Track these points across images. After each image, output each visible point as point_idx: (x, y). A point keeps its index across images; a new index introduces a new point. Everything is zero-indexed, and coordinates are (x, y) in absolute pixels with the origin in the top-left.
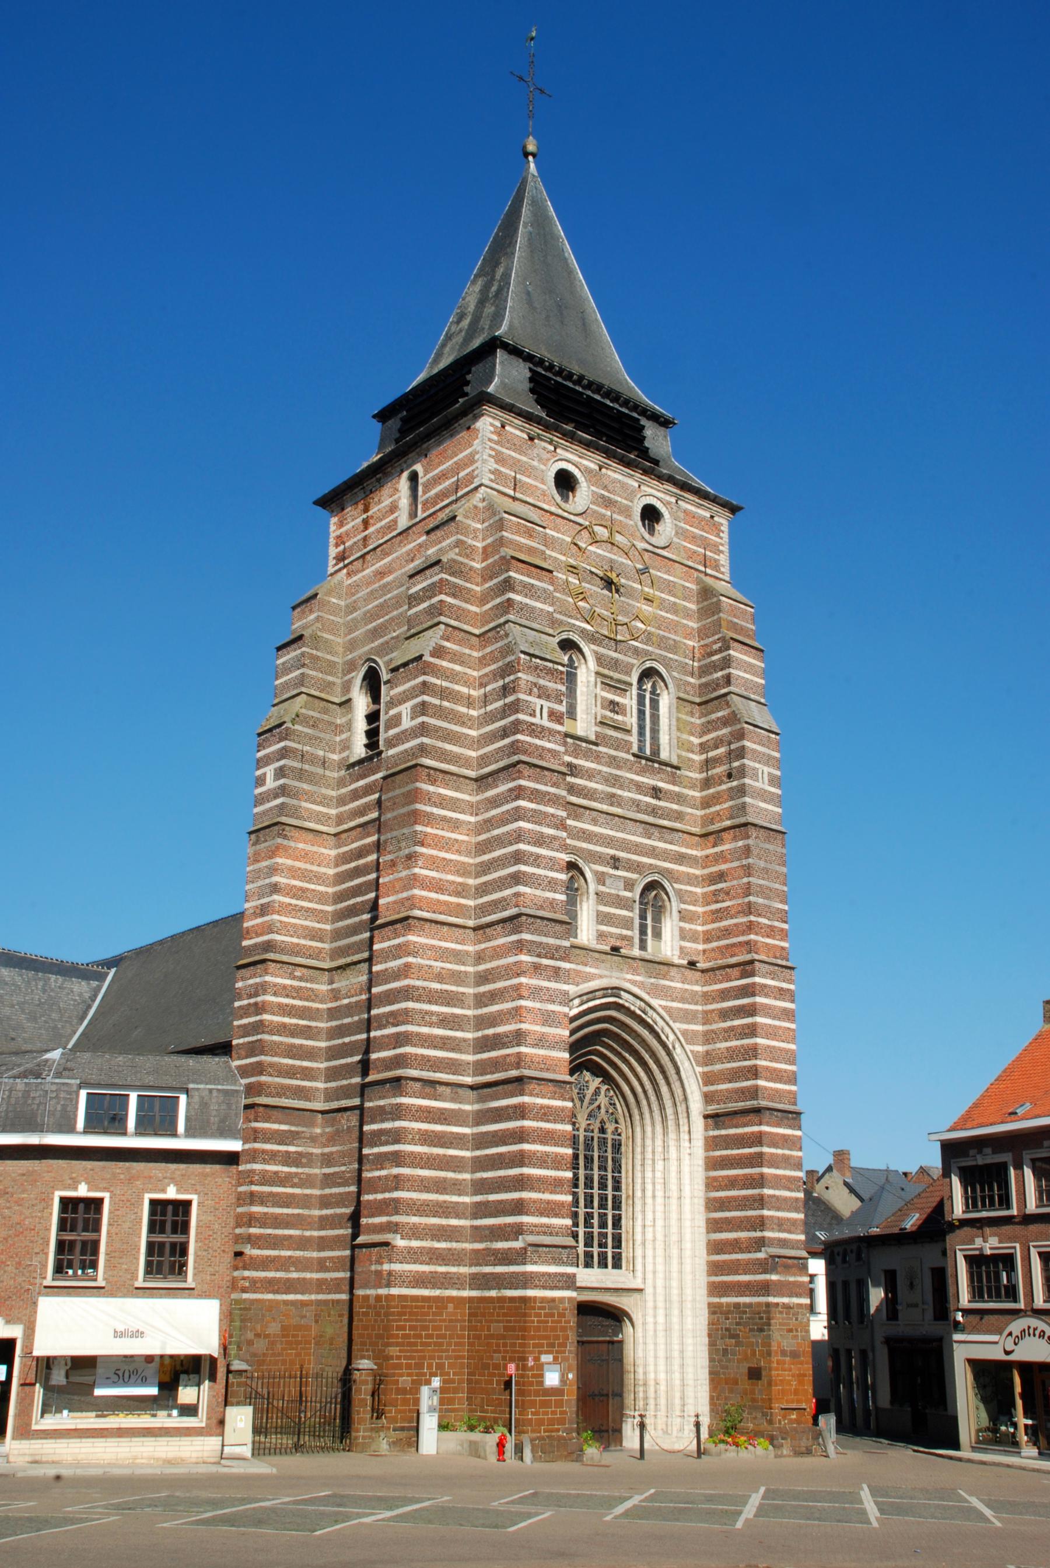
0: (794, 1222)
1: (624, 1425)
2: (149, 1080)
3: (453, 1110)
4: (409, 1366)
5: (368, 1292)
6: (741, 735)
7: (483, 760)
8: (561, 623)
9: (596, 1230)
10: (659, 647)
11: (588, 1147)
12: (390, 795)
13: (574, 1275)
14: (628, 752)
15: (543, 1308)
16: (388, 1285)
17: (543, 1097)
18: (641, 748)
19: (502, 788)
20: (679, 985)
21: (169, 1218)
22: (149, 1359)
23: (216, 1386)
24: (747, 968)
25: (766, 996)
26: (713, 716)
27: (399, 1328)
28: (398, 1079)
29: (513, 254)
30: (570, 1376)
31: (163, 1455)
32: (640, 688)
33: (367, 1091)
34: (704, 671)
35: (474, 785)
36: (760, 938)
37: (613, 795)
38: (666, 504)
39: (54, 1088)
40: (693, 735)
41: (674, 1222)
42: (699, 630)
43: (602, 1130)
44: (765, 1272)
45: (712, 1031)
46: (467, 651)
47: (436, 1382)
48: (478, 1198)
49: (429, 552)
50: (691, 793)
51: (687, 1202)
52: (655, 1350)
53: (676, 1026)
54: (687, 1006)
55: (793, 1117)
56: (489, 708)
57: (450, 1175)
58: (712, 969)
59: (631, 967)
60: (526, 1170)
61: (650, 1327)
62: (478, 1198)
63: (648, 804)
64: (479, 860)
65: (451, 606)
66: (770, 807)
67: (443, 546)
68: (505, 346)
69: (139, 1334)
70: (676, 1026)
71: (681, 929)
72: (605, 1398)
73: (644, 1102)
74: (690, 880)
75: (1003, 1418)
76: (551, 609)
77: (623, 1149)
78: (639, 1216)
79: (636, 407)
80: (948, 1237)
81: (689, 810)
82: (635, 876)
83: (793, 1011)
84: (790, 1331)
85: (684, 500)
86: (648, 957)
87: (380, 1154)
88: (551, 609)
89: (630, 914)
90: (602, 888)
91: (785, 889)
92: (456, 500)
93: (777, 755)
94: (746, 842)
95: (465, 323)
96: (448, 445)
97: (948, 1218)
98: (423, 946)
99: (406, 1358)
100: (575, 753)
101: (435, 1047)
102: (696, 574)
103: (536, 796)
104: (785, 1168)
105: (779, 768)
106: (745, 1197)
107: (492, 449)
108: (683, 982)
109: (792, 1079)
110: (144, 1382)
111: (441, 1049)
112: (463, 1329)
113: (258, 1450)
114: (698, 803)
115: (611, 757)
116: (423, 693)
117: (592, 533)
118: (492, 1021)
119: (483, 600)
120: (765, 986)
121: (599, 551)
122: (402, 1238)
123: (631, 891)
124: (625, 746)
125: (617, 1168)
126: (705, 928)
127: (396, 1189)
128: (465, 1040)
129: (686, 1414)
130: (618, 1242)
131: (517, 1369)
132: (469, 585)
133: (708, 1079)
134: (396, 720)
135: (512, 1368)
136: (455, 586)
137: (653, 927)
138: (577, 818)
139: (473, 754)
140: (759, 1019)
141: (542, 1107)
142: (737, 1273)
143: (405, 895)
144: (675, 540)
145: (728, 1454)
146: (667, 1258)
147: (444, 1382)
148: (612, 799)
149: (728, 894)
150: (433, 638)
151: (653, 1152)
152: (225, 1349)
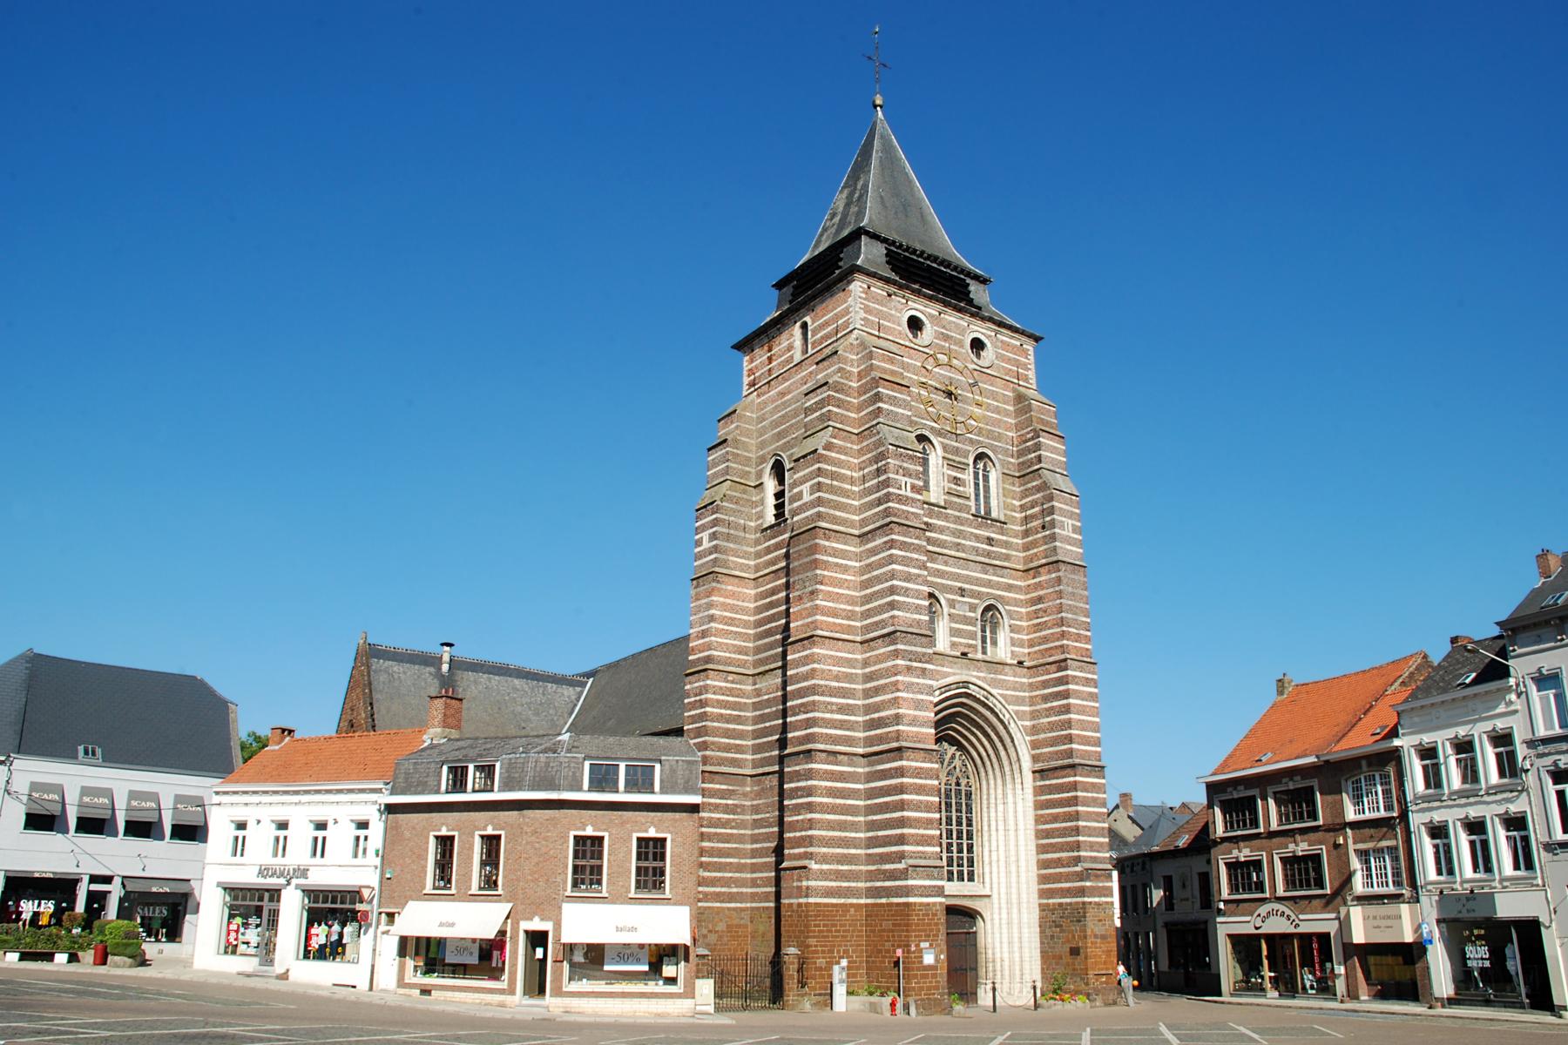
0: (1101, 844)
2: (633, 754)
3: (850, 772)
4: (823, 952)
5: (792, 901)
6: (1051, 498)
7: (864, 522)
8: (916, 423)
9: (955, 855)
10: (988, 438)
11: (948, 796)
12: (796, 549)
13: (943, 887)
14: (968, 513)
15: (921, 910)
16: (807, 896)
18: (978, 509)
19: (879, 541)
20: (1012, 679)
21: (651, 850)
22: (641, 946)
23: (689, 965)
24: (1062, 664)
25: (1077, 684)
26: (1029, 485)
27: (815, 926)
28: (809, 751)
29: (870, 171)
30: (942, 957)
31: (655, 1010)
32: (975, 467)
33: (786, 760)
34: (1021, 454)
35: (858, 540)
36: (1070, 643)
37: (959, 544)
38: (988, 337)
39: (566, 760)
40: (1014, 499)
41: (1012, 847)
42: (1016, 425)
43: (958, 784)
44: (1082, 880)
45: (1037, 711)
46: (849, 445)
47: (844, 963)
48: (871, 834)
49: (819, 377)
50: (1015, 540)
51: (1021, 833)
52: (1001, 938)
53: (1010, 708)
54: (1017, 693)
55: (1099, 770)
56: (867, 485)
57: (849, 818)
58: (1036, 667)
59: (976, 667)
60: (906, 814)
61: (997, 922)
62: (871, 834)
63: (984, 550)
64: (863, 593)
65: (837, 414)
66: (1074, 549)
67: (829, 372)
68: (867, 233)
69: (633, 929)
70: (1010, 708)
71: (1012, 638)
73: (988, 763)
74: (1017, 603)
75: (1252, 973)
76: (910, 413)
77: (973, 796)
78: (986, 844)
79: (962, 271)
80: (1212, 851)
81: (1014, 553)
82: (976, 601)
83: (1096, 694)
84: (1100, 921)
85: (1001, 333)
86: (989, 659)
87: (797, 804)
88: (910, 413)
89: (974, 629)
90: (953, 611)
91: (1087, 606)
92: (837, 340)
93: (1077, 511)
94: (1058, 574)
95: (837, 219)
96: (830, 303)
97: (1212, 837)
98: (824, 656)
99: (821, 946)
100: (930, 515)
101: (836, 728)
102: (1012, 385)
103: (904, 546)
104: (1094, 806)
105: (1079, 521)
106: (1065, 828)
107: (861, 303)
109: (1097, 743)
110: (638, 961)
111: (840, 729)
112: (861, 925)
113: (718, 1009)
114: (1020, 547)
115: (955, 516)
116: (819, 476)
117: (936, 359)
118: (877, 708)
119: (859, 409)
120: (1075, 677)
121: (942, 372)
122: (816, 863)
123: (974, 612)
124: (967, 509)
125: (969, 810)
126: (1029, 637)
127: (810, 829)
128: (857, 722)
130: (971, 862)
131: (903, 953)
132: (848, 399)
133: (1035, 745)
134: (799, 496)
135: (899, 952)
136: (839, 399)
137: (991, 638)
138: (933, 561)
139: (857, 518)
140: (1071, 701)
141: (916, 768)
142: (1060, 882)
143: (810, 620)
144: (996, 362)
145: (1056, 1007)
146: (1008, 873)
147: (849, 962)
148: (958, 546)
149: (1045, 612)
150: (825, 436)
151: (996, 799)
152: (695, 940)
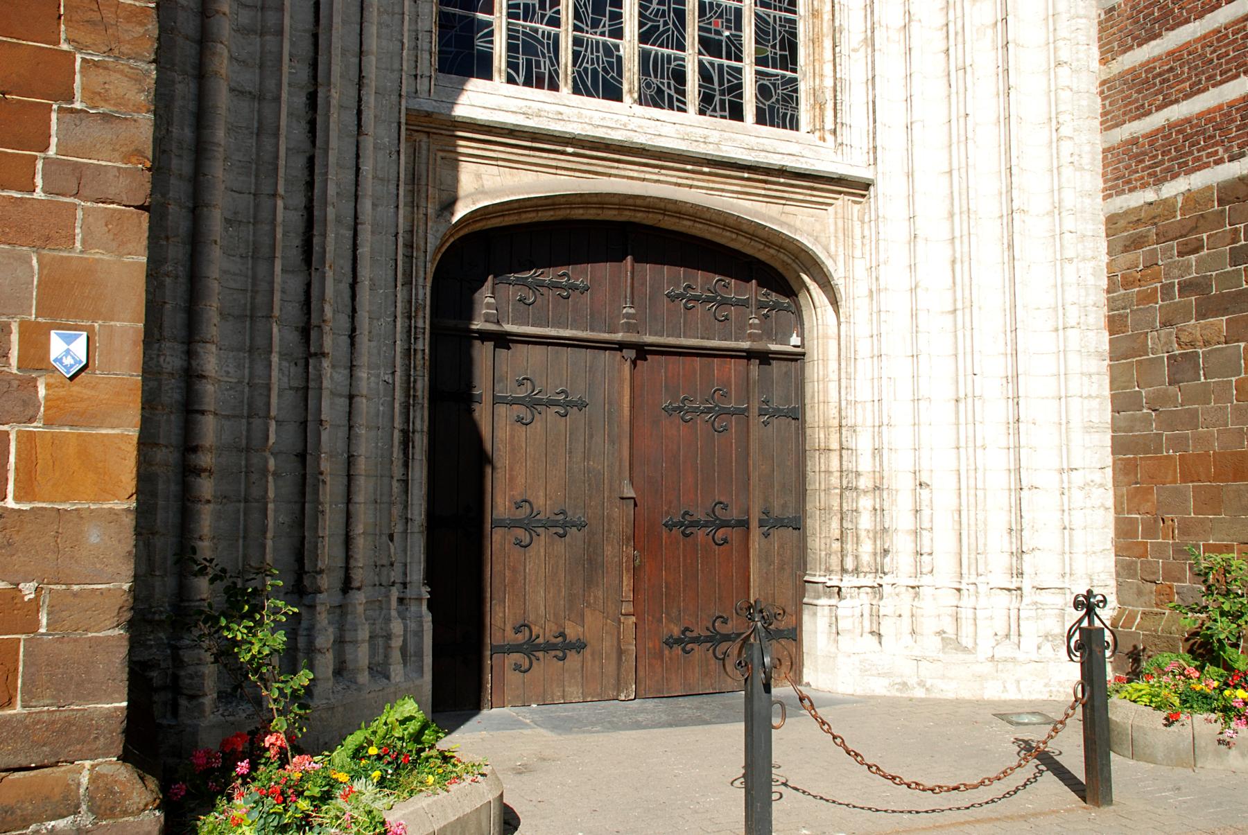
1: (806, 618)
72: (735, 534)
129: (1027, 585)
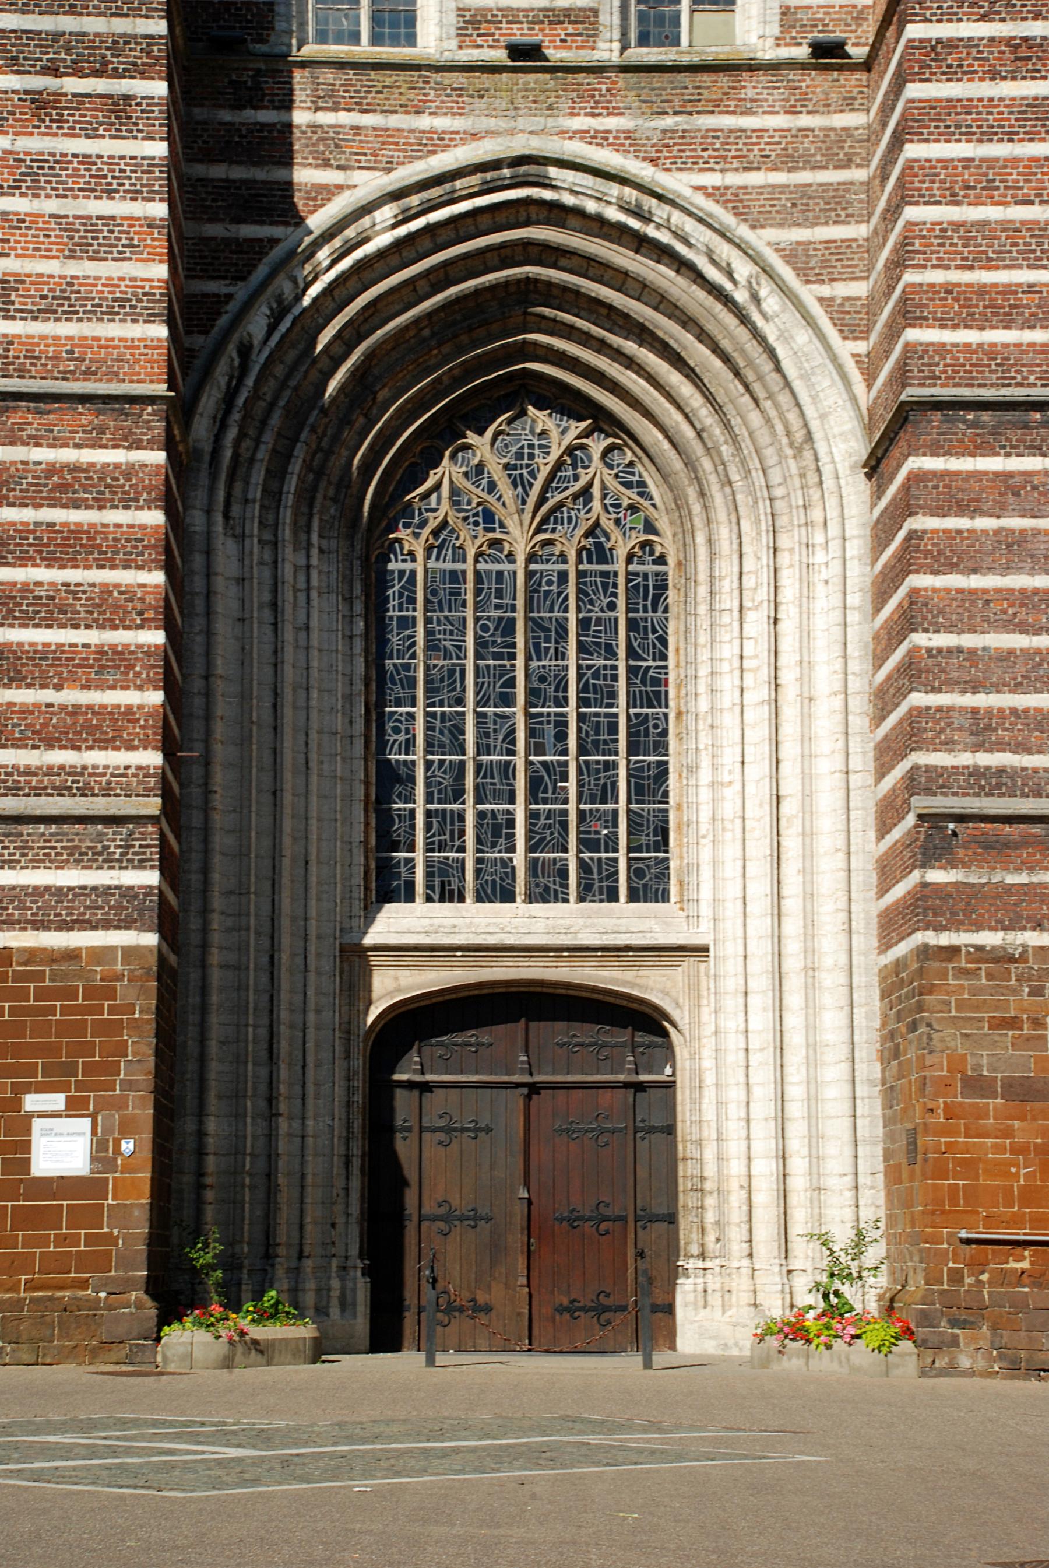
17: (56, 443)
53: (761, 239)
70: (761, 239)
86: (686, 59)
108: (792, 111)
